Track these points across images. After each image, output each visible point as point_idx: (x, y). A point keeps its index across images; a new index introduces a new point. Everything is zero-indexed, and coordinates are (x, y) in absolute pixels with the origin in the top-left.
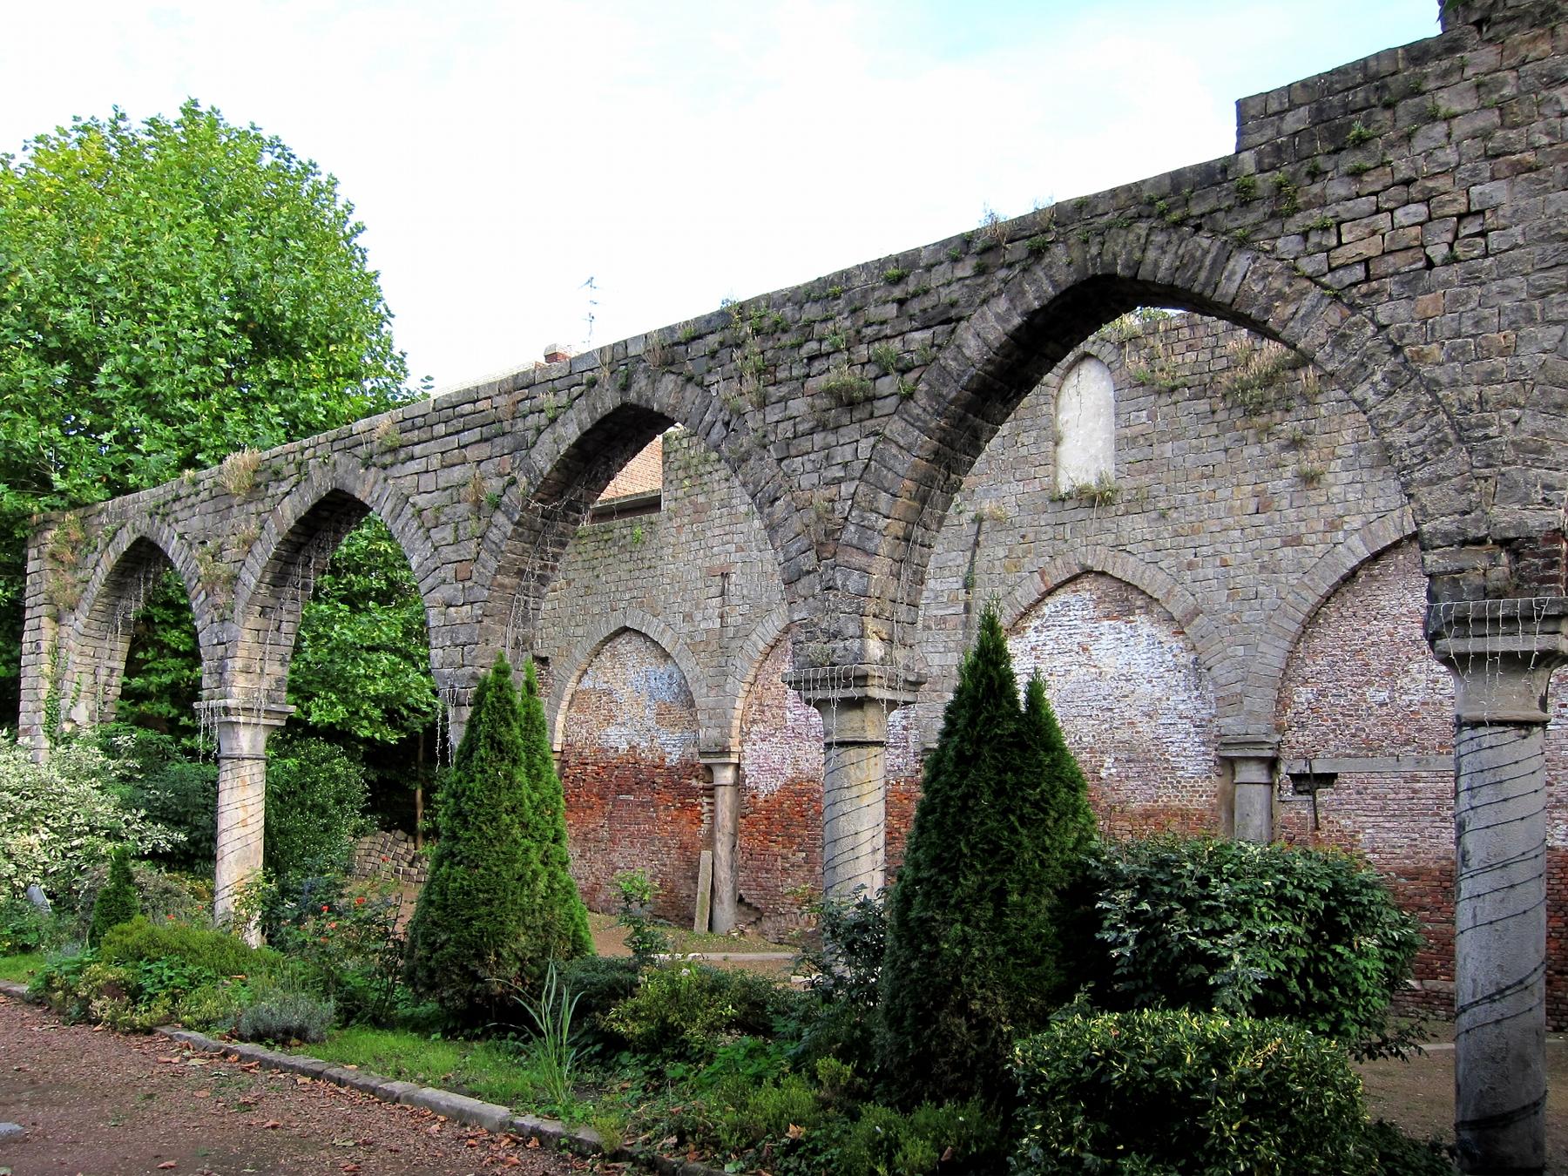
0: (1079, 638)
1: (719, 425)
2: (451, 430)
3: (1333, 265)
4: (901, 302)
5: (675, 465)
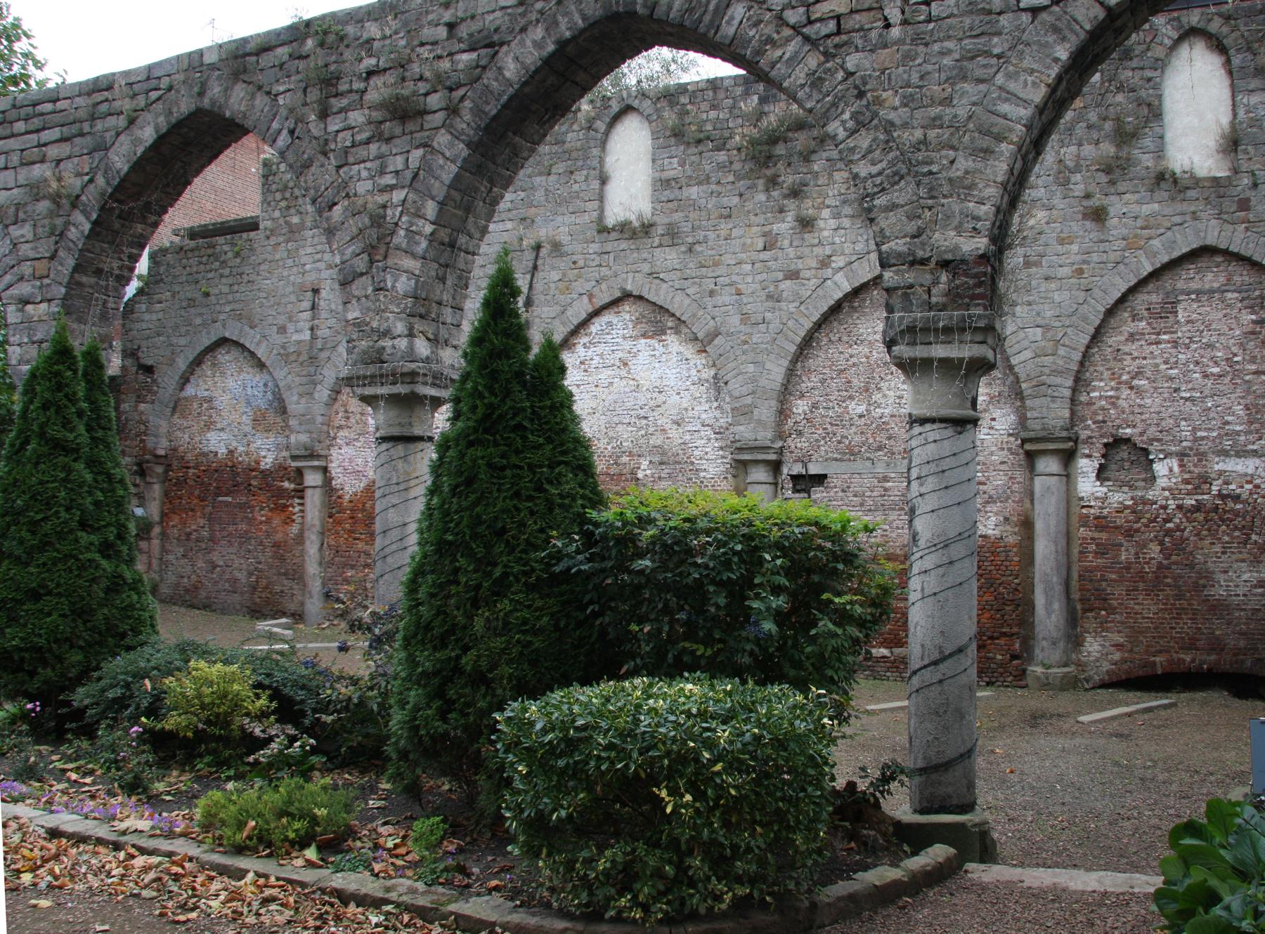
0: (620, 355)
1: (285, 132)
2: (32, 128)
3: (813, 18)
4: (451, 26)
5: (274, 187)
